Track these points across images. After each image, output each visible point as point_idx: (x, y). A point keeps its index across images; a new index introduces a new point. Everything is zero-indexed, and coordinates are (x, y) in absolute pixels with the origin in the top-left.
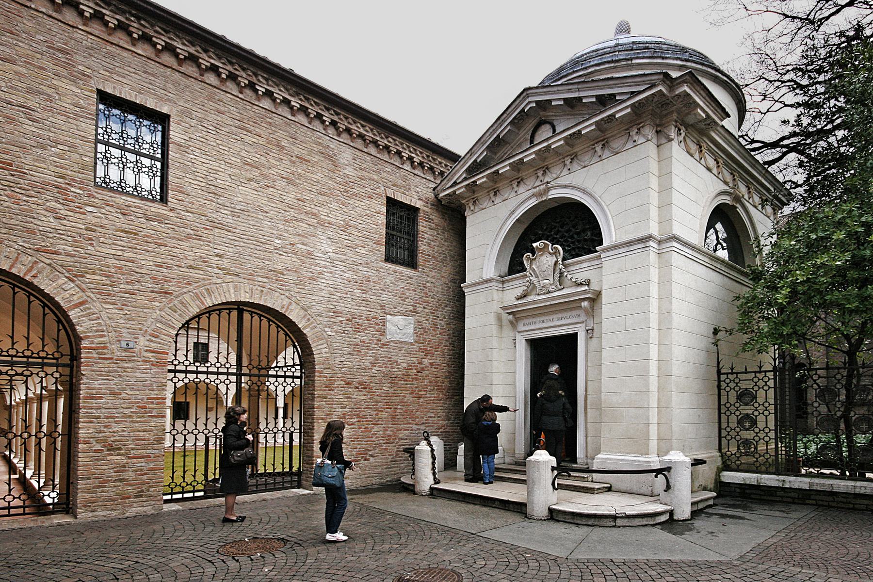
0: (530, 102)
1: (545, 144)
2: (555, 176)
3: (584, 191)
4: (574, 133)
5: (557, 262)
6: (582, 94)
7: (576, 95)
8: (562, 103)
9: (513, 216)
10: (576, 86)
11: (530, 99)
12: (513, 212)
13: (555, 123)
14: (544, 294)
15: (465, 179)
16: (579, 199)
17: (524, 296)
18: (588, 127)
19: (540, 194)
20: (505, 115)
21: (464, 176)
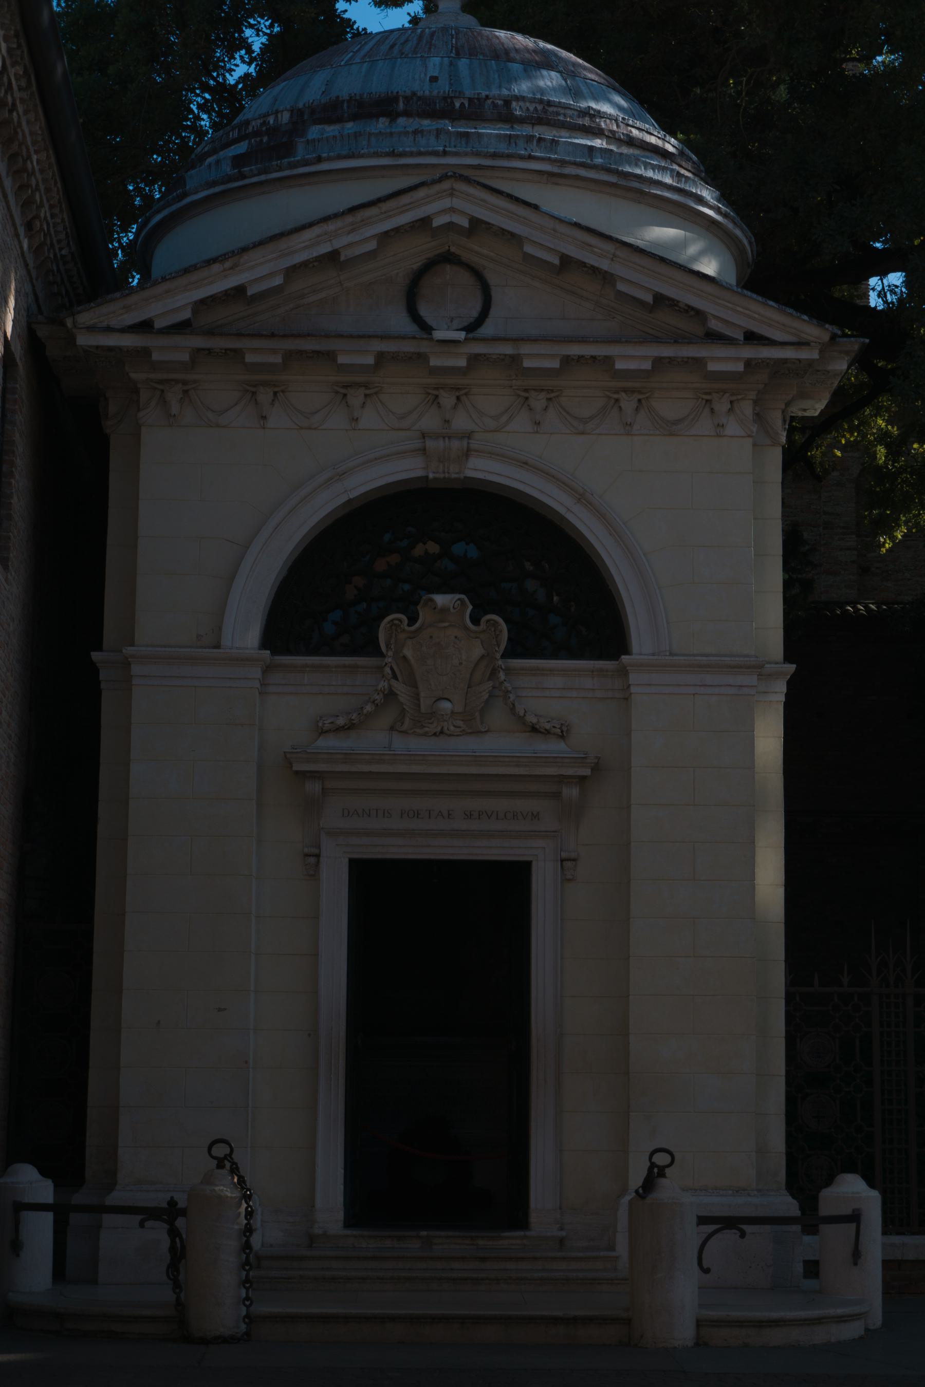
0: (452, 210)
1: (508, 349)
3: (582, 498)
4: (594, 358)
5: (483, 657)
6: (618, 270)
7: (604, 265)
8: (556, 261)
10: (609, 247)
11: (457, 203)
13: (492, 278)
14: (425, 734)
15: (182, 327)
16: (562, 511)
17: (350, 727)
18: (633, 358)
20: (373, 211)
21: (187, 314)
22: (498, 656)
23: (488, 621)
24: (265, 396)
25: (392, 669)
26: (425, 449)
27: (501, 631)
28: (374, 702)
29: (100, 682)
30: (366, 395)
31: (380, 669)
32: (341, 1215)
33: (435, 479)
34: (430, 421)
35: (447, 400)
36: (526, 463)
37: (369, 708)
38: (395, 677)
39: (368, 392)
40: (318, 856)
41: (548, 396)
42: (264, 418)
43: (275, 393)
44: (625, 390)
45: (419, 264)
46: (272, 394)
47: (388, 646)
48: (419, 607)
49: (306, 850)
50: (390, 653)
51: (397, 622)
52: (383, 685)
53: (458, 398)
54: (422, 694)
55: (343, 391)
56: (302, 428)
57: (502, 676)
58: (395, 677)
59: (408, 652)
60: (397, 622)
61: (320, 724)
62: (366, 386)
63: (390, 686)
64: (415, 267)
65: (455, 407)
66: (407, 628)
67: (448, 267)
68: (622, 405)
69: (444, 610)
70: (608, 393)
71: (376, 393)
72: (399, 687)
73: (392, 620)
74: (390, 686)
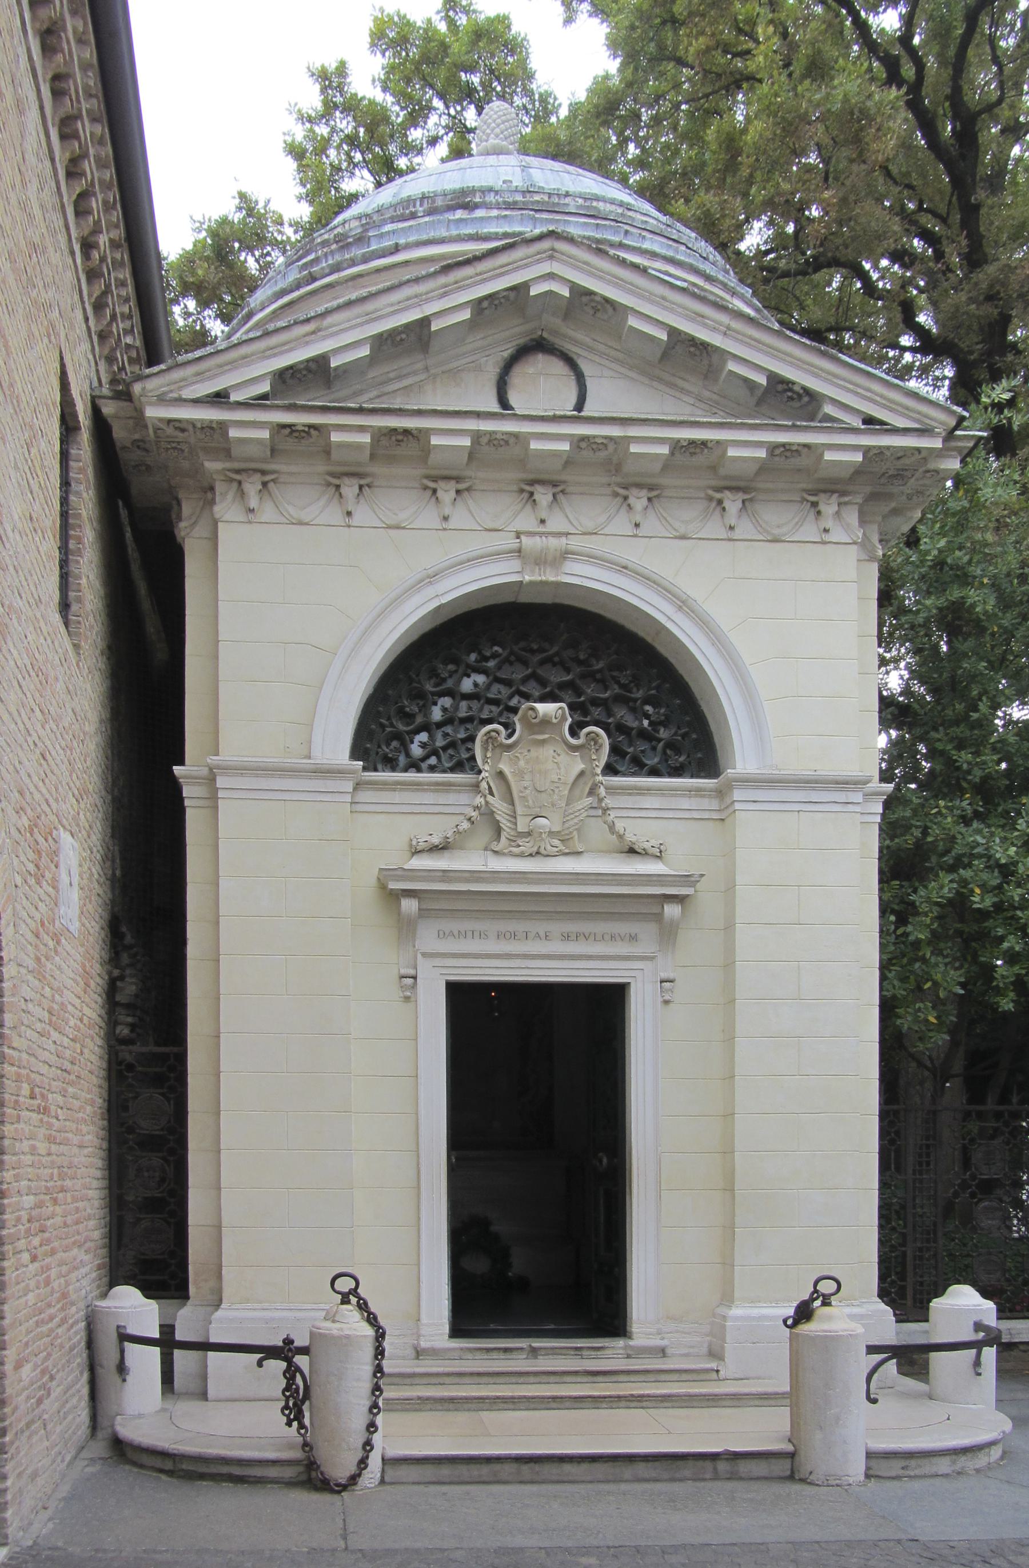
2: (589, 525)
3: (683, 604)
5: (582, 773)
9: (430, 591)
12: (432, 577)
19: (540, 560)
22: (599, 771)
23: (589, 734)
24: (350, 489)
25: (488, 783)
26: (519, 551)
27: (601, 746)
28: (469, 819)
29: (181, 799)
30: (458, 492)
31: (477, 786)
32: (446, 1329)
33: (532, 583)
34: (526, 521)
35: (544, 496)
36: (625, 568)
37: (466, 825)
38: (491, 793)
39: (461, 486)
40: (415, 978)
41: (650, 495)
42: (349, 514)
43: (361, 487)
44: (729, 488)
45: (509, 351)
46: (357, 487)
47: (485, 762)
48: (516, 719)
49: (403, 971)
50: (487, 767)
51: (493, 734)
52: (479, 800)
53: (554, 495)
54: (520, 810)
55: (432, 485)
56: (389, 527)
57: (602, 791)
58: (491, 793)
59: (505, 767)
60: (493, 734)
61: (414, 843)
62: (458, 479)
63: (487, 803)
64: (506, 354)
65: (550, 506)
66: (504, 741)
67: (540, 357)
68: (727, 504)
69: (545, 723)
70: (710, 492)
71: (468, 489)
72: (497, 803)
73: (489, 732)
74: (487, 803)
